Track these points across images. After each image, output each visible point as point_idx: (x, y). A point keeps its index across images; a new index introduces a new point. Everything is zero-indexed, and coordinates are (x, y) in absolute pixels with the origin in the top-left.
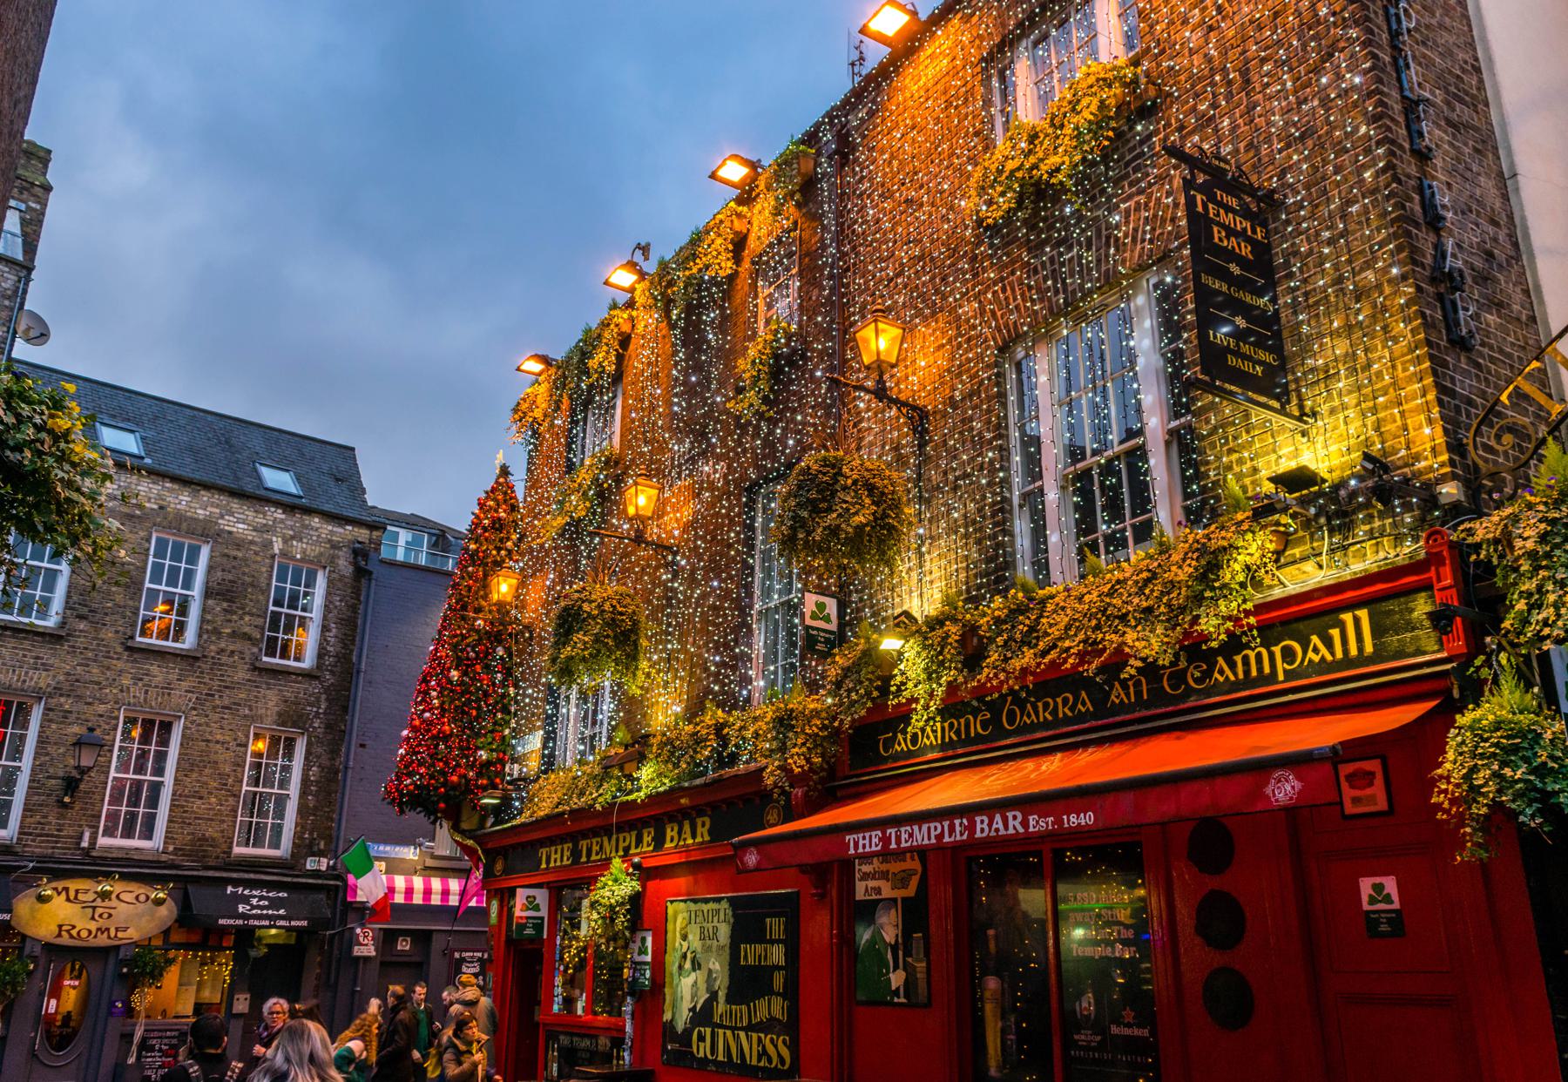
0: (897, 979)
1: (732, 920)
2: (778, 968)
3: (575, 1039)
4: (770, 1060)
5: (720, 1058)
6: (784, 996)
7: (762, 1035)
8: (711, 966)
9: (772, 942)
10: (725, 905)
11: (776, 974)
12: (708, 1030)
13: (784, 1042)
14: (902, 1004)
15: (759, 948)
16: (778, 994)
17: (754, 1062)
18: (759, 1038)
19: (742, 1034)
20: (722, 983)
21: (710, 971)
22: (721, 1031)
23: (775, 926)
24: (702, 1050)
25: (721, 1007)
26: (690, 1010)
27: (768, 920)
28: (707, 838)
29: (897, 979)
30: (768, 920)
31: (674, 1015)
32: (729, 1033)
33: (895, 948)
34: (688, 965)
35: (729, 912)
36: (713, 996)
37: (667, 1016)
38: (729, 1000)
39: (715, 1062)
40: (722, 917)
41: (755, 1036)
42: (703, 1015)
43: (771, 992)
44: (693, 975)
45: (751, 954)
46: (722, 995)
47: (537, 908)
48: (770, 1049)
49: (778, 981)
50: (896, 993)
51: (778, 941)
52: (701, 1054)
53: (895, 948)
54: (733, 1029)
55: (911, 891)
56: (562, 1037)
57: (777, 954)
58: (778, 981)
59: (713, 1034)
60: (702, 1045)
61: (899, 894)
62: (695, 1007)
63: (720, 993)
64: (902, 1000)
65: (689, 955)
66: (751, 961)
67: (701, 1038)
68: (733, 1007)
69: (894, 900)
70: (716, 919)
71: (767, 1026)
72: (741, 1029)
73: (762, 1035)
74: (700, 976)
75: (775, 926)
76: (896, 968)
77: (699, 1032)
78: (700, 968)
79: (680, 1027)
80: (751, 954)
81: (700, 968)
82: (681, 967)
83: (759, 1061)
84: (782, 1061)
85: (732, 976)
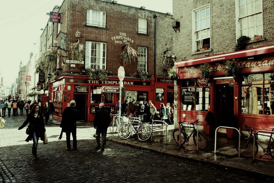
0: (161, 99)
10: (136, 92)
15: (142, 96)
20: (135, 98)
21: (133, 98)
28: (133, 84)
29: (161, 99)
33: (161, 97)
34: (129, 97)
35: (137, 92)
38: (137, 101)
44: (130, 99)
45: (141, 97)
49: (145, 99)
53: (161, 97)
55: (163, 92)
57: (145, 97)
58: (145, 99)
61: (161, 93)
74: (132, 99)
75: (145, 94)
78: (131, 98)
80: (141, 97)
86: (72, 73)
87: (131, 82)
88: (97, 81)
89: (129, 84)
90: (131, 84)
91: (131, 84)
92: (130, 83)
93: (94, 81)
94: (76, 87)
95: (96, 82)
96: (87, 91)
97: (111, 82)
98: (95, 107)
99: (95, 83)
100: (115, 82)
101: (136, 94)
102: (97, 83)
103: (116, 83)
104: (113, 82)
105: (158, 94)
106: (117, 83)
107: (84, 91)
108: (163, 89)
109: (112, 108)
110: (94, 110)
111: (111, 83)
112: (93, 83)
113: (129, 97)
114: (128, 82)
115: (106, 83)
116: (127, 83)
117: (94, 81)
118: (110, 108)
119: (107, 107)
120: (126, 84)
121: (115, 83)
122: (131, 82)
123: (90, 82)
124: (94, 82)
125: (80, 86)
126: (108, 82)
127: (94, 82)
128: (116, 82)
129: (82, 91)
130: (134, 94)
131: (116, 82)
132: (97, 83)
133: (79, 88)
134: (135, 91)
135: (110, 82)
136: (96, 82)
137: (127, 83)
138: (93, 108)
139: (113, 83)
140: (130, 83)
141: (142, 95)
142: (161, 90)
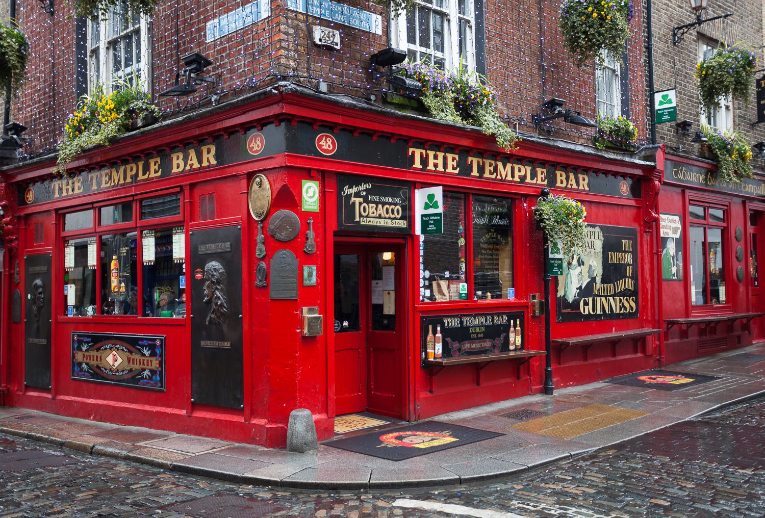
0: (674, 270)
1: (603, 239)
2: (629, 265)
3: (464, 319)
4: (626, 309)
5: (599, 312)
6: (632, 278)
7: (622, 298)
8: (591, 263)
9: (626, 252)
10: (597, 229)
11: (628, 268)
12: (591, 299)
13: (633, 300)
14: (675, 280)
16: (629, 277)
17: (618, 312)
18: (620, 300)
19: (611, 299)
20: (598, 272)
21: (590, 266)
22: (599, 299)
23: (627, 244)
24: (586, 310)
25: (598, 285)
26: (577, 289)
27: (623, 241)
28: (587, 188)
29: (674, 270)
30: (623, 241)
31: (565, 292)
32: (603, 299)
33: (673, 257)
34: (575, 262)
36: (593, 280)
37: (560, 293)
38: (603, 281)
39: (596, 316)
40: (596, 236)
41: (618, 299)
42: (586, 291)
43: (625, 276)
45: (614, 258)
46: (598, 279)
47: (435, 206)
48: (626, 304)
49: (629, 271)
50: (674, 275)
51: (629, 252)
52: (587, 312)
53: (673, 257)
54: (606, 297)
55: (678, 236)
56: (446, 321)
57: (628, 259)
58: (629, 271)
59: (594, 301)
60: (586, 307)
62: (581, 286)
63: (597, 278)
64: (676, 278)
65: (575, 256)
66: (615, 261)
67: (586, 304)
68: (606, 285)
69: (673, 238)
70: (592, 237)
71: (623, 294)
72: (610, 296)
73: (622, 298)
74: (585, 269)
76: (674, 265)
77: (585, 300)
78: (583, 264)
79: (571, 299)
80: (614, 258)
81: (583, 264)
82: (569, 264)
83: (620, 310)
84: (632, 309)
85: (604, 269)
86: (323, 87)
87: (581, 176)
88: (450, 156)
89: (575, 186)
90: (581, 187)
91: (581, 187)
92: (578, 183)
93: (436, 157)
94: (347, 191)
95: (445, 165)
96: (403, 224)
97: (509, 166)
98: (443, 325)
99: (440, 168)
100: (522, 173)
101: (599, 245)
102: (450, 170)
103: (528, 180)
104: (516, 167)
105: (665, 240)
106: (532, 179)
107: (390, 223)
108: (677, 218)
109: (515, 326)
110: (439, 347)
111: (509, 178)
112: (431, 167)
113: (575, 262)
114: (572, 176)
115: (487, 175)
116: (567, 178)
117: (436, 157)
118: (507, 328)
119: (497, 320)
120: (564, 185)
121: (525, 176)
122: (581, 176)
123: (418, 164)
124: (436, 165)
125: (369, 186)
126: (496, 169)
127: (436, 165)
128: (529, 169)
129: (382, 223)
130: (592, 246)
131: (529, 169)
132: (450, 170)
133: (366, 201)
134: (594, 227)
135: (505, 167)
136: (445, 165)
137: (567, 178)
138: (435, 332)
139: (517, 179)
140: (578, 183)
141: (618, 248)
142: (673, 225)
